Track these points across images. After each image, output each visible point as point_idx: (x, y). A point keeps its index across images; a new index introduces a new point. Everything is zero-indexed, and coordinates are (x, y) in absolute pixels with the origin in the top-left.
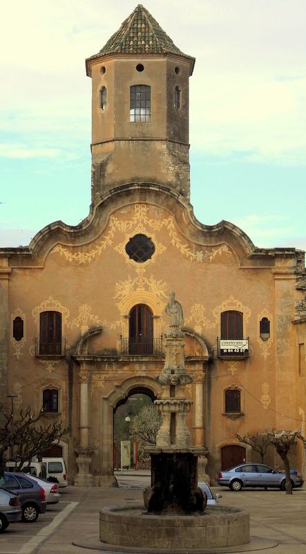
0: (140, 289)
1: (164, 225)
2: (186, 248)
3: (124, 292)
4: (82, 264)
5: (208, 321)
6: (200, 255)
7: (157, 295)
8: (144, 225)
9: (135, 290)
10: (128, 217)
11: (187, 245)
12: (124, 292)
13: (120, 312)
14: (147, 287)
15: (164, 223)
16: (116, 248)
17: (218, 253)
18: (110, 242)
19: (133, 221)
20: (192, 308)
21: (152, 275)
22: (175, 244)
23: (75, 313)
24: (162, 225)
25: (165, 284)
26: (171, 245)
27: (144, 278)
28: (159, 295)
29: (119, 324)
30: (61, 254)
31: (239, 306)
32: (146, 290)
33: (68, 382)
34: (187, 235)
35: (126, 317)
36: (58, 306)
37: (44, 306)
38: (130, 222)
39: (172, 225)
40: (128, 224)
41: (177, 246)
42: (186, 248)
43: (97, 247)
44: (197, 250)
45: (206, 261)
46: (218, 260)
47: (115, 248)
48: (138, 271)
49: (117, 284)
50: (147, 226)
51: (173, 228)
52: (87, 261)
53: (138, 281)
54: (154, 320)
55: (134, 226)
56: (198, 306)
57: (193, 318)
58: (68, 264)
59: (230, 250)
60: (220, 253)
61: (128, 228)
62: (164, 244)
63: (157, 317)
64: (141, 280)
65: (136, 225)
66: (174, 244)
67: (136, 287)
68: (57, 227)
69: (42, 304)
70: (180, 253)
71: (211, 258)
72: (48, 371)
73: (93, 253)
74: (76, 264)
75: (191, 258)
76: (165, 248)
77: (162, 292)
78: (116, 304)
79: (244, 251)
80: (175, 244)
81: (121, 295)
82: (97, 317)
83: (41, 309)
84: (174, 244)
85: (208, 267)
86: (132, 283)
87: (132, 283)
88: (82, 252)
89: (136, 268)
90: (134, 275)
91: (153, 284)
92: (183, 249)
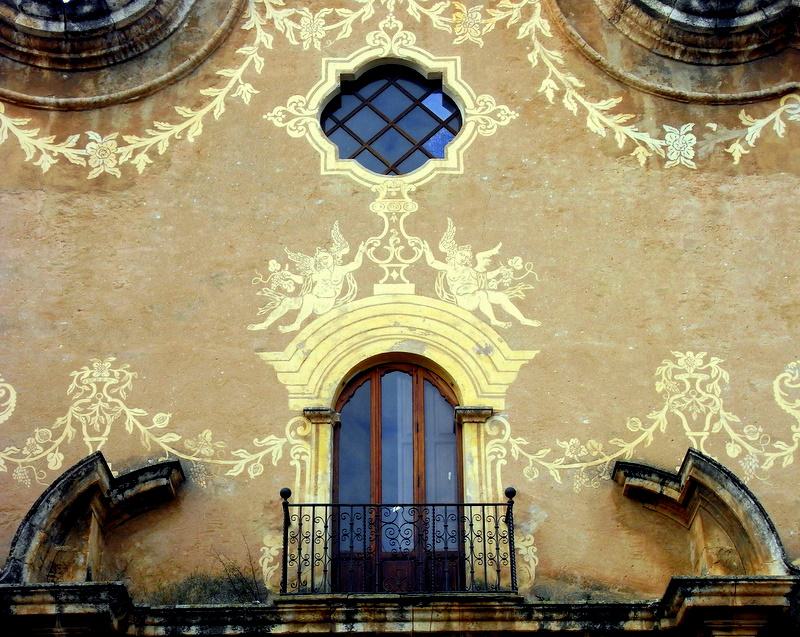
0: (392, 288)
1: (501, 24)
2: (614, 112)
3: (308, 304)
4: (103, 179)
5: (753, 432)
6: (681, 142)
7: (477, 313)
8: (410, 25)
9: (365, 292)
11: (613, 102)
12: (308, 304)
13: (283, 394)
14: (425, 280)
15: (498, 15)
16: (275, 117)
17: (767, 130)
18: (247, 92)
20: (660, 370)
21: (451, 230)
22: (560, 95)
24: (491, 25)
26: (541, 100)
27: (412, 240)
28: (489, 312)
29: (277, 453)
32: (418, 292)
34: (614, 56)
35: (314, 415)
38: (340, 11)
40: (333, 19)
41: (569, 104)
42: (614, 112)
43: (181, 110)
44: (663, 119)
45: (713, 163)
47: (268, 117)
48: (379, 207)
49: (273, 265)
50: (423, 30)
51: (546, 29)
52: (127, 169)
53: (381, 254)
54: (469, 431)
55: (361, 29)
56: (690, 361)
57: (673, 421)
58: (31, 178)
60: (780, 128)
61: (332, 34)
62: (506, 96)
63: (482, 415)
64: (394, 251)
65: (372, 24)
66: (550, 96)
67: (368, 278)
70: (583, 132)
71: (737, 150)
73: (161, 137)
74: (73, 180)
75: (641, 154)
76: (508, 115)
77: (502, 299)
78: (267, 356)
80: (560, 95)
81: (290, 317)
82: (161, 420)
84: (550, 96)
85: (723, 188)
86: (348, 259)
87: (348, 259)
88: (104, 130)
89: (375, 195)
90: (360, 224)
91: (457, 266)
92: (600, 117)
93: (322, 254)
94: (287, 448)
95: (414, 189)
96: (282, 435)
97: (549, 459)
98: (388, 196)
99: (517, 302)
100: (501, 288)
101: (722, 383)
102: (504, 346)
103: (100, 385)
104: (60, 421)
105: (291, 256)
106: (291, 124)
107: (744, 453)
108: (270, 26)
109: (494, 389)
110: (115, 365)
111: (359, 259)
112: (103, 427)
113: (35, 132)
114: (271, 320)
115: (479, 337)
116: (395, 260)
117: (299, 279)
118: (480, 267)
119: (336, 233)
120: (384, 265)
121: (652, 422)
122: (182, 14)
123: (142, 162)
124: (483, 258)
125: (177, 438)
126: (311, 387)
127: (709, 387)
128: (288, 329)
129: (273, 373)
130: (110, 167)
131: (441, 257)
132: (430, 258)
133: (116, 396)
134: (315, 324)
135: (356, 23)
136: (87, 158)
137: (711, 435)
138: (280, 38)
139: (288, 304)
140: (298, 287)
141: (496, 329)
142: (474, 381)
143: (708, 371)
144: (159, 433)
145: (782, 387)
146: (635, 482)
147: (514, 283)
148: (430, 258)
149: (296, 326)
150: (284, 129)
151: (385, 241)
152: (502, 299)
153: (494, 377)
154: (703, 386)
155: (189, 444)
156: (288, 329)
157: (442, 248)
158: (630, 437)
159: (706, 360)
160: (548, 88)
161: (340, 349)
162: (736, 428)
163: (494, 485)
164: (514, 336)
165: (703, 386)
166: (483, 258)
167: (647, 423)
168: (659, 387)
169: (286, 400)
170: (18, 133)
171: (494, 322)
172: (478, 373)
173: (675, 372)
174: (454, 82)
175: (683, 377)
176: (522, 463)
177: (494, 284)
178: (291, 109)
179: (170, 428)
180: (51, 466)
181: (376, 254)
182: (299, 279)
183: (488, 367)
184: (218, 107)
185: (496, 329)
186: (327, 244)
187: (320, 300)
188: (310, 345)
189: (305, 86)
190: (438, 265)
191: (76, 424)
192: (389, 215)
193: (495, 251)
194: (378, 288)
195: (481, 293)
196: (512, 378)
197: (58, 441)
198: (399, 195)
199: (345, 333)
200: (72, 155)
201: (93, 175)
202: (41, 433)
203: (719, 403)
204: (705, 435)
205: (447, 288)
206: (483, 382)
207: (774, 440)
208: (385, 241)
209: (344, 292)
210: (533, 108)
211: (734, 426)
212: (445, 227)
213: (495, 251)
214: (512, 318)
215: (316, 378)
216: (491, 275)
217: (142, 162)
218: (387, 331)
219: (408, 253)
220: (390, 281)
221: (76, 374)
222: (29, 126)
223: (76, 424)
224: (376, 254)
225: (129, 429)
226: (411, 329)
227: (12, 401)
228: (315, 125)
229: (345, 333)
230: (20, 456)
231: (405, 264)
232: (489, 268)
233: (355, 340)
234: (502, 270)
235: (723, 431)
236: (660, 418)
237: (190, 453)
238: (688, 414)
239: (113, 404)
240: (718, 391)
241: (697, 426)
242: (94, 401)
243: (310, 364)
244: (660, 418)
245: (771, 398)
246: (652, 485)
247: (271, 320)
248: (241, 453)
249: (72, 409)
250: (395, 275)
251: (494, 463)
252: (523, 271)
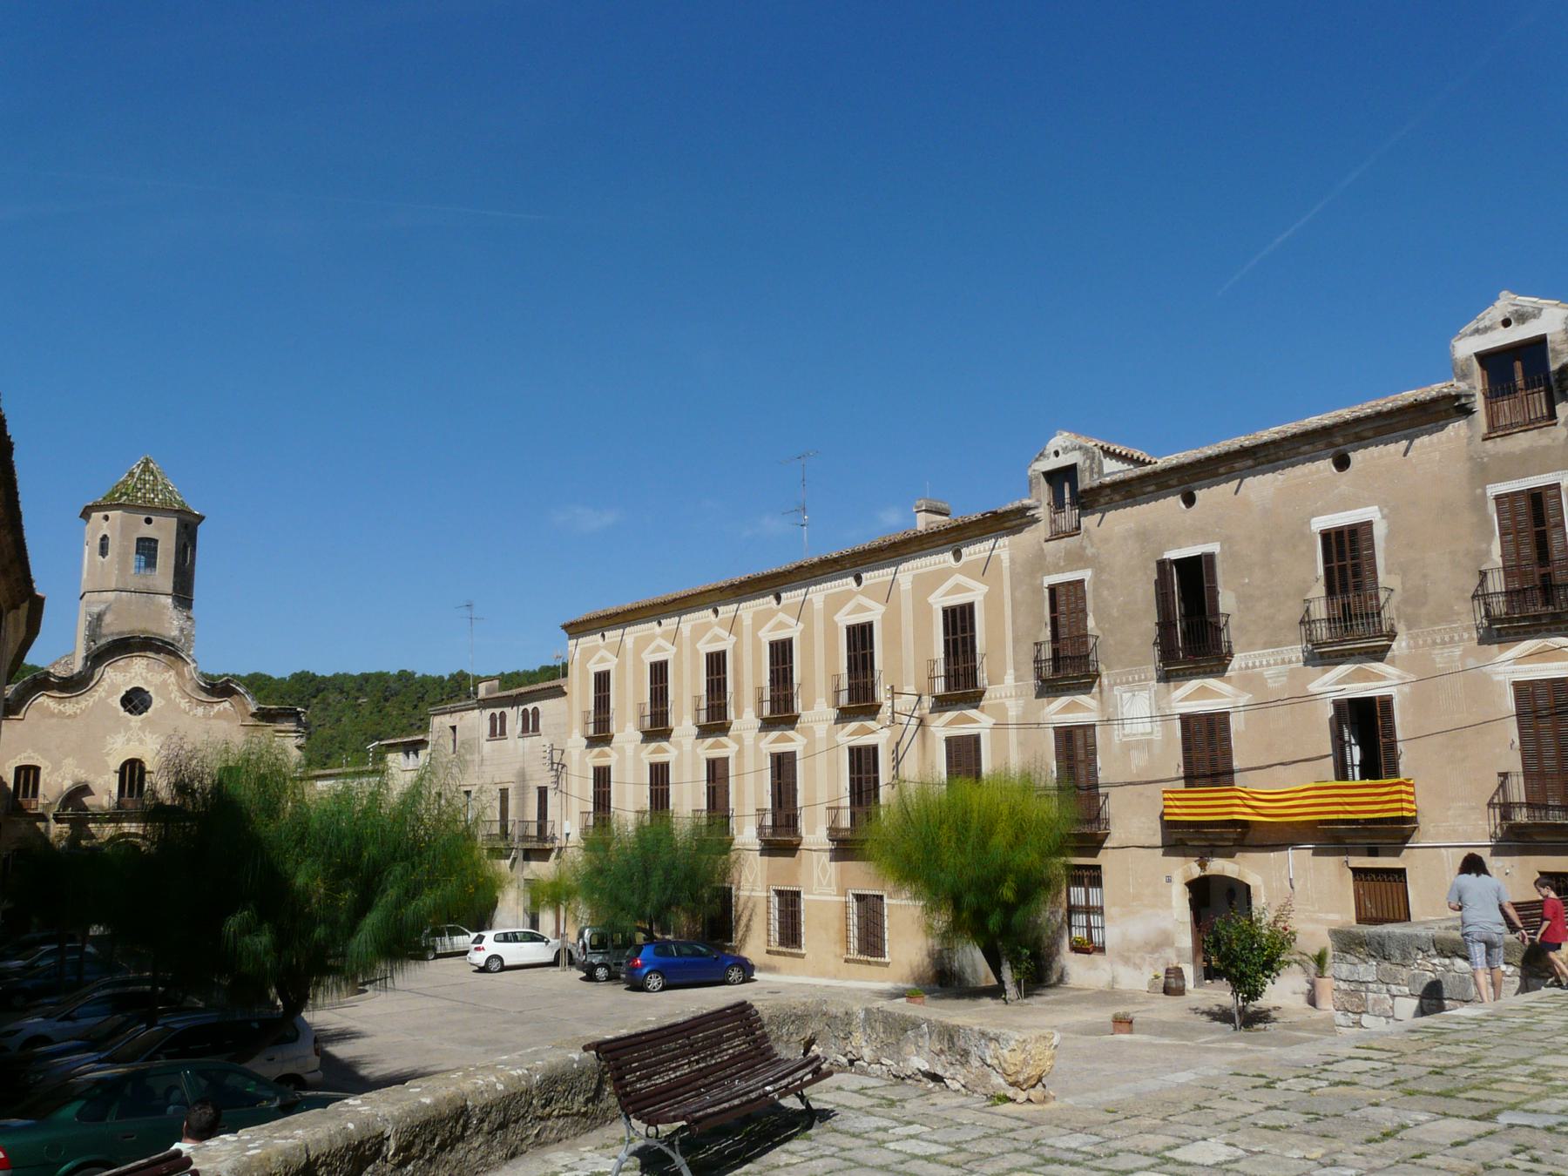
4: (70, 715)
6: (200, 711)
8: (143, 678)
10: (125, 670)
14: (141, 741)
16: (109, 700)
23: (57, 766)
35: (116, 772)
39: (173, 679)
41: (177, 701)
45: (206, 717)
46: (218, 716)
50: (145, 679)
58: (53, 715)
59: (232, 706)
67: (129, 740)
69: (19, 757)
70: (179, 707)
73: (83, 705)
74: (61, 715)
76: (163, 702)
79: (246, 708)
82: (82, 772)
90: (128, 728)
92: (184, 704)
108: (110, 677)
123: (78, 711)
138: (112, 681)
139: (110, 747)
160: (173, 696)
184: (96, 698)
187: (118, 746)
200: (63, 709)
202: (57, 774)
210: (169, 701)
217: (78, 711)
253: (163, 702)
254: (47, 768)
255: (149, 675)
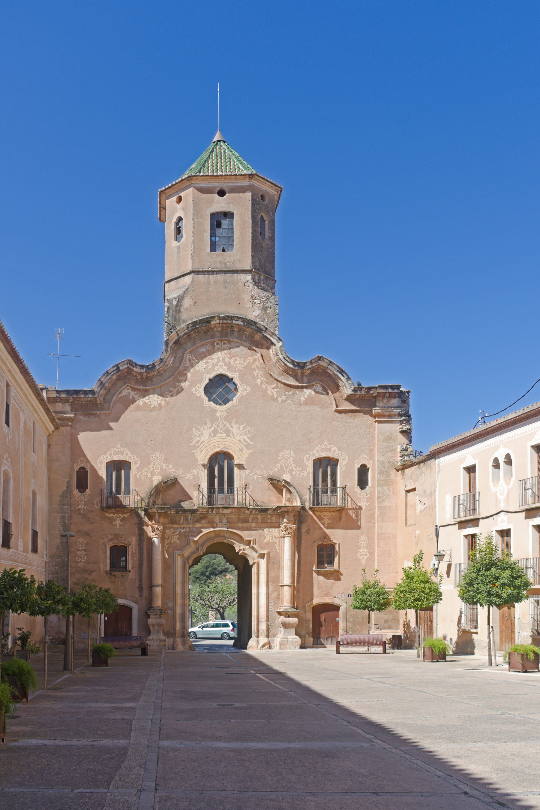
3: (202, 438)
4: (155, 407)
9: (215, 435)
12: (202, 438)
13: (196, 460)
14: (228, 433)
19: (213, 359)
21: (234, 420)
25: (249, 428)
27: (225, 423)
28: (243, 441)
29: (196, 473)
30: (131, 397)
31: (335, 451)
32: (227, 436)
33: (138, 539)
35: (203, 465)
36: (127, 454)
37: (111, 455)
43: (172, 389)
49: (194, 429)
52: (160, 405)
53: (218, 426)
57: (282, 466)
67: (215, 432)
68: (126, 366)
69: (109, 453)
72: (116, 525)
77: (245, 437)
78: (193, 451)
81: (198, 442)
82: (171, 466)
83: (107, 457)
86: (211, 428)
91: (235, 429)
93: (205, 427)
94: (198, 472)
95: (226, 409)
96: (197, 470)
97: (254, 475)
98: (220, 412)
99: (248, 438)
100: (245, 435)
101: (293, 457)
102: (245, 449)
103: (157, 458)
104: (149, 466)
105: (198, 427)
106: (197, 392)
107: (296, 473)
109: (242, 459)
110: (160, 454)
111: (213, 427)
112: (159, 468)
113: (138, 395)
114: (194, 443)
115: (240, 447)
116: (221, 428)
117: (200, 433)
118: (241, 429)
119: (208, 422)
120: (219, 429)
121: (277, 466)
122: (171, 362)
124: (241, 427)
125: (174, 470)
126: (203, 459)
127: (290, 458)
128: (196, 445)
129: (194, 455)
130: (156, 404)
131: (232, 427)
132: (229, 427)
133: (161, 461)
134: (203, 444)
135: (213, 363)
136: (150, 402)
137: (290, 469)
139: (197, 439)
140: (199, 434)
141: (244, 444)
142: (239, 457)
143: (290, 454)
144: (170, 469)
145: (306, 458)
146: (272, 482)
147: (248, 433)
148: (229, 427)
149: (199, 444)
150: (195, 393)
151: (219, 423)
152: (245, 437)
153: (243, 456)
154: (289, 458)
155: (177, 472)
156: (196, 445)
157: (232, 425)
158: (272, 470)
159: (290, 452)
161: (209, 450)
162: (295, 468)
163: (242, 481)
164: (248, 446)
165: (289, 458)
166: (241, 427)
167: (276, 467)
168: (279, 458)
169: (197, 462)
170: (134, 395)
171: (243, 443)
172: (240, 456)
173: (283, 455)
174: (236, 380)
175: (285, 456)
176: (248, 476)
177: (244, 434)
178: (197, 388)
179: (173, 468)
180: (148, 477)
181: (217, 426)
182: (200, 433)
183: (242, 454)
185: (244, 444)
186: (206, 424)
188: (202, 449)
189: (200, 382)
190: (231, 429)
191: (153, 467)
192: (220, 416)
193: (244, 425)
194: (218, 435)
195: (241, 436)
196: (247, 456)
197: (149, 471)
198: (223, 411)
199: (210, 446)
201: (152, 406)
202: (146, 469)
203: (292, 462)
204: (288, 469)
205: (233, 435)
206: (241, 457)
207: (303, 470)
208: (219, 423)
209: (210, 436)
211: (295, 467)
212: (233, 419)
213: (244, 425)
214: (247, 442)
215: (203, 457)
216: (243, 431)
218: (219, 445)
219: (224, 426)
220: (220, 433)
221: (152, 456)
222: (137, 394)
223: (153, 467)
224: (217, 426)
225: (164, 468)
226: (225, 445)
227: (139, 462)
228: (203, 392)
229: (210, 446)
230: (142, 474)
231: (224, 429)
232: (243, 430)
233: (213, 447)
234: (246, 430)
235: (292, 469)
236: (279, 466)
237: (177, 474)
238: (285, 465)
239: (160, 463)
240: (292, 459)
241: (287, 467)
242: (156, 462)
243: (203, 453)
244: (279, 466)
245: (304, 461)
246: (276, 482)
247: (194, 443)
248: (188, 474)
249: (152, 464)
250: (221, 431)
251: (242, 476)
252: (250, 430)
253: (249, 389)
254: (136, 463)
255: (232, 361)
